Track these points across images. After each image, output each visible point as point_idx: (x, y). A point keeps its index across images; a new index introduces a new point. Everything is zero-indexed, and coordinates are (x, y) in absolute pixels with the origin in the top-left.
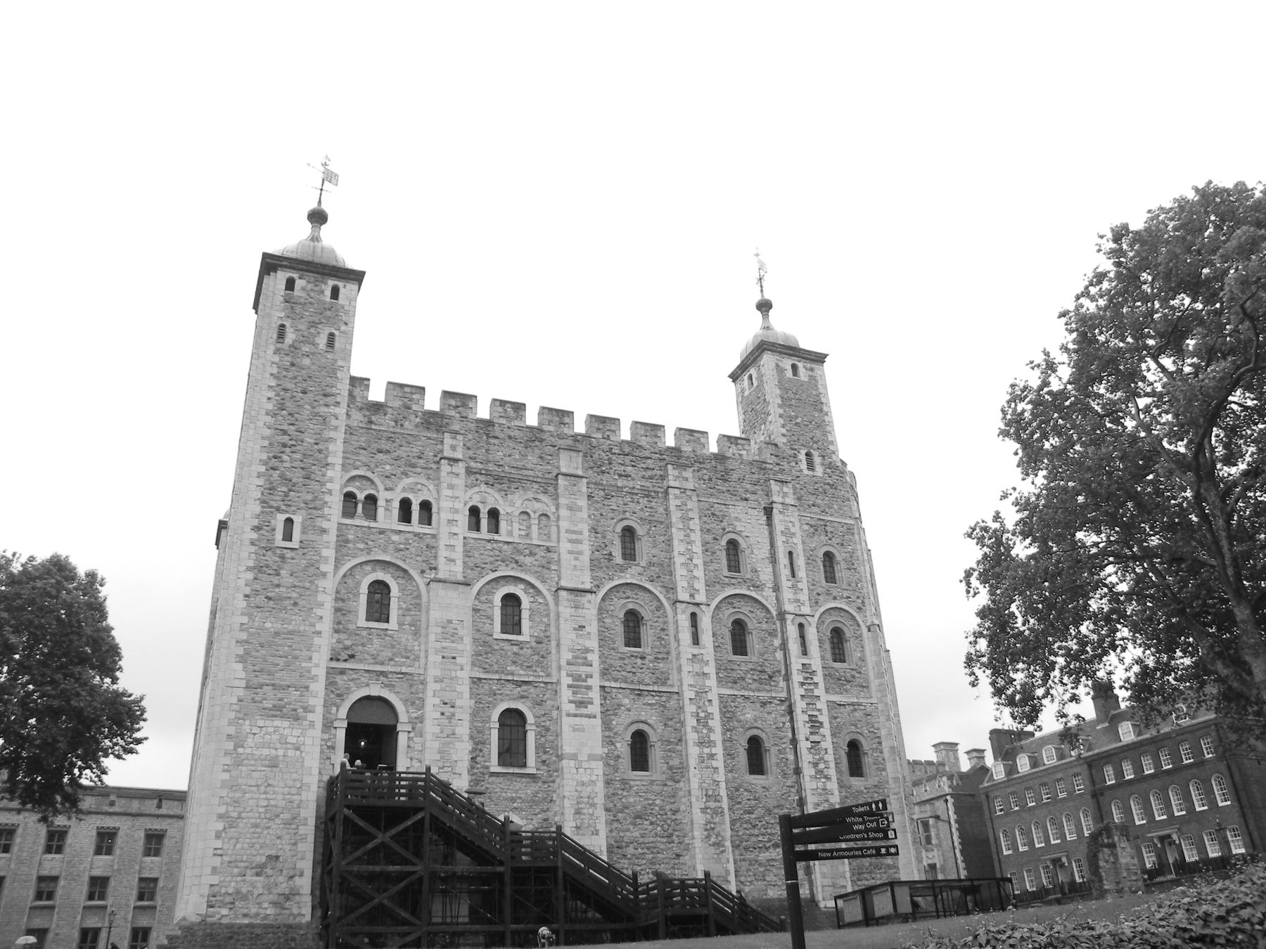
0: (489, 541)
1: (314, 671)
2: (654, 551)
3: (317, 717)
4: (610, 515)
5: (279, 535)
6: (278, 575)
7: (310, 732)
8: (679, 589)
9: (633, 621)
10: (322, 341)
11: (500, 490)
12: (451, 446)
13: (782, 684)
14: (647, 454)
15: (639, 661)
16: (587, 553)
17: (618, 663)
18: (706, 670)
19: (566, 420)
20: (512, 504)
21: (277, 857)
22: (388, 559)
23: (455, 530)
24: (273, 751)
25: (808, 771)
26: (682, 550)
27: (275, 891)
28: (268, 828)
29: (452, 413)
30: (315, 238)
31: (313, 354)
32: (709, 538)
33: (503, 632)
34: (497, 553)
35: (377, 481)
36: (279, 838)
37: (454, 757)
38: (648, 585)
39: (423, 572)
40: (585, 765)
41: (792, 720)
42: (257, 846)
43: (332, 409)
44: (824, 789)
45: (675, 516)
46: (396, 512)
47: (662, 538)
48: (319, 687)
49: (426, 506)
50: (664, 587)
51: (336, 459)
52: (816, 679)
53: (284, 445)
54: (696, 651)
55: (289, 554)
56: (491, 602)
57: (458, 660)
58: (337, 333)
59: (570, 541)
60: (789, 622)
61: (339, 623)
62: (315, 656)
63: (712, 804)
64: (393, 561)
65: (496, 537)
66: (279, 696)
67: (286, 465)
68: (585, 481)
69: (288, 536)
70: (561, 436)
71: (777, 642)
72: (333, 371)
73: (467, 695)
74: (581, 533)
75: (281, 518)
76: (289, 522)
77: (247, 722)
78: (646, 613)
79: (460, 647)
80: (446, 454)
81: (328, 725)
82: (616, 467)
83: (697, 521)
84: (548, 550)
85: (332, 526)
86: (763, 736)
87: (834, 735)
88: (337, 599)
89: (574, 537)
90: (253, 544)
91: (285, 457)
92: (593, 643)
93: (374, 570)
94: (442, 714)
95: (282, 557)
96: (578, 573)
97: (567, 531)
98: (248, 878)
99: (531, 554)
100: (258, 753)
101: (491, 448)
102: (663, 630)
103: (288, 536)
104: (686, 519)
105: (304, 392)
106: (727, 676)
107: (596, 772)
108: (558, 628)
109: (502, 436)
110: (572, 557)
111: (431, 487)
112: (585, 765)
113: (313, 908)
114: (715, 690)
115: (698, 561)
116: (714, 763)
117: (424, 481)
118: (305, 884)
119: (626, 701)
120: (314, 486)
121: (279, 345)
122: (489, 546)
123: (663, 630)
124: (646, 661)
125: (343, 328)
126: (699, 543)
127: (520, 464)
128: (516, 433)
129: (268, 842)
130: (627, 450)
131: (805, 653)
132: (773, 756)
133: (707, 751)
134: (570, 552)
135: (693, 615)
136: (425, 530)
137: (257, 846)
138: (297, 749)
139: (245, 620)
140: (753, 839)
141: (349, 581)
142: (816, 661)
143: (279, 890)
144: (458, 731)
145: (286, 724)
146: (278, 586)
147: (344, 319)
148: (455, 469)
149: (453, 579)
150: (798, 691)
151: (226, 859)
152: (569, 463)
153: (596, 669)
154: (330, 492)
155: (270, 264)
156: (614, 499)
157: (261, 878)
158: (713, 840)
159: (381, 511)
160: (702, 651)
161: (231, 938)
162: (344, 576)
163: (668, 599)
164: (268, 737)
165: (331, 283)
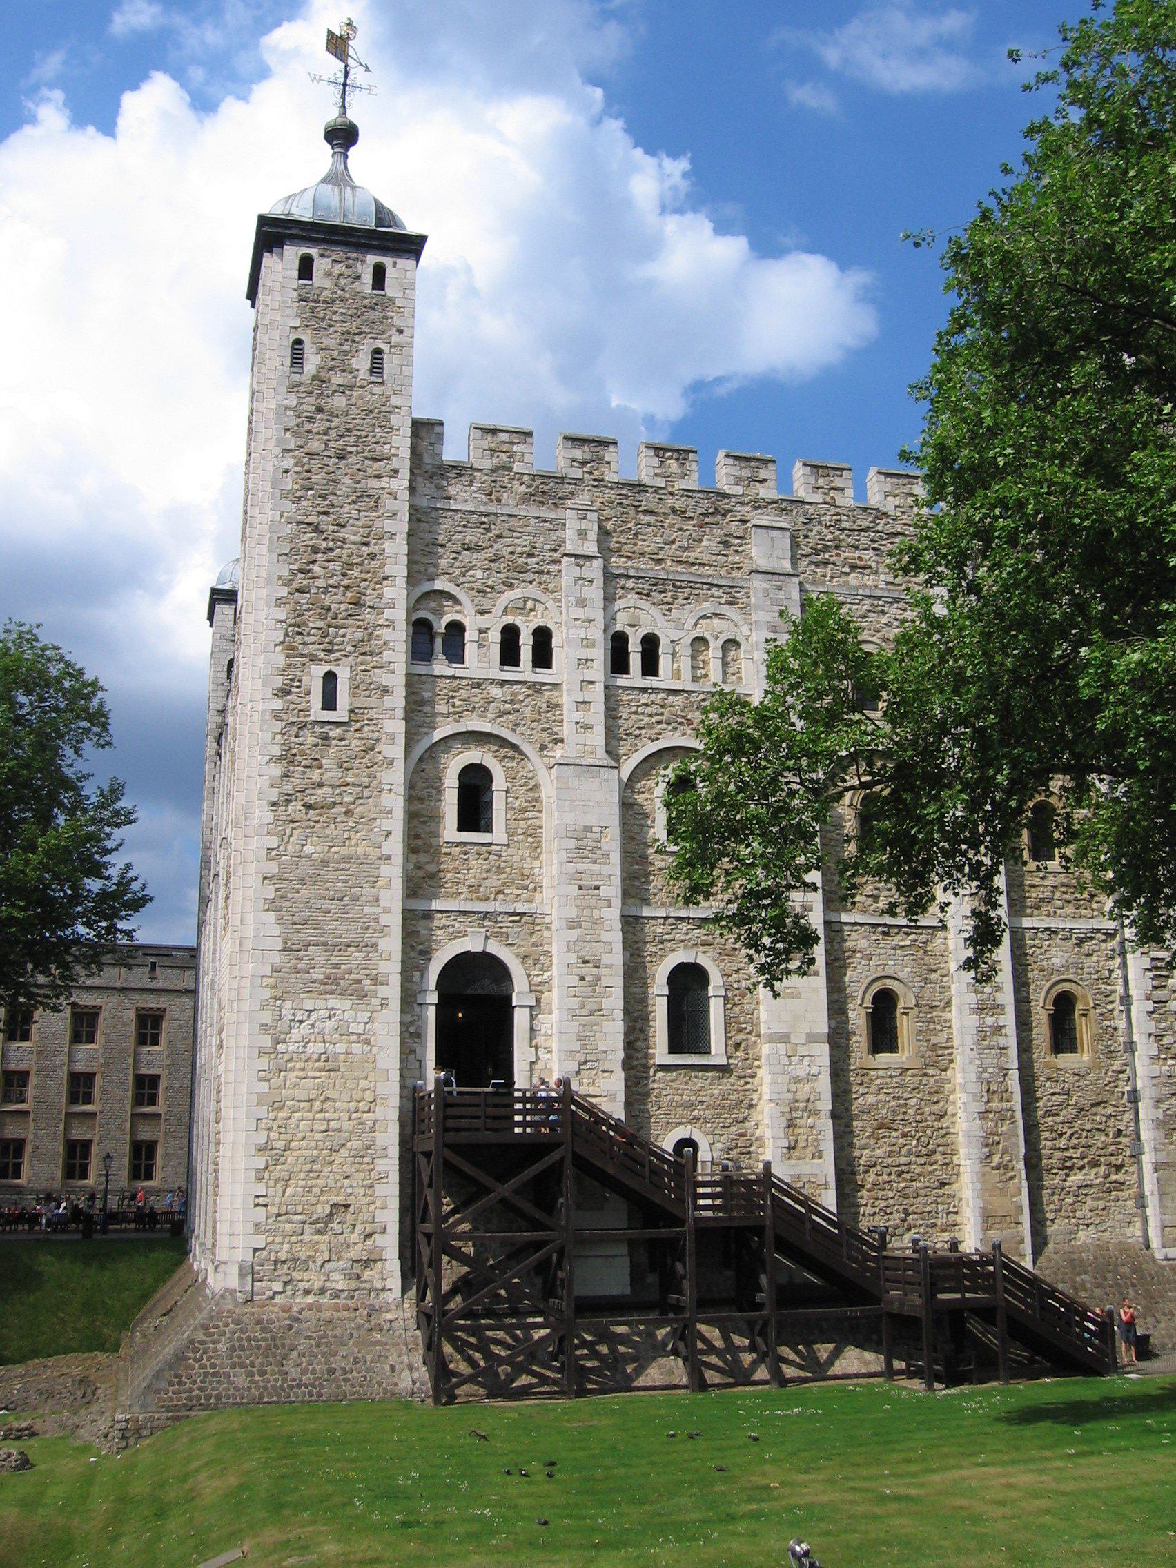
1: (384, 919)
3: (392, 991)
5: (316, 700)
6: (320, 767)
10: (362, 363)
21: (347, 1206)
27: (348, 1256)
29: (578, 473)
30: (339, 178)
31: (351, 388)
37: (602, 1046)
40: (802, 1051)
43: (385, 482)
46: (496, 651)
49: (543, 638)
51: (398, 568)
53: (315, 550)
55: (335, 732)
57: (604, 891)
58: (385, 347)
61: (417, 837)
62: (384, 895)
63: (995, 1105)
64: (496, 730)
67: (320, 582)
68: (796, 580)
69: (329, 702)
70: (757, 505)
72: (381, 416)
73: (618, 947)
75: (319, 671)
76: (330, 678)
77: (288, 1004)
79: (606, 869)
80: (569, 548)
81: (410, 999)
85: (397, 681)
90: (278, 718)
91: (317, 569)
94: (582, 979)
95: (326, 738)
98: (306, 1237)
101: (645, 530)
103: (329, 702)
105: (341, 457)
107: (819, 1061)
111: (550, 604)
112: (802, 1051)
116: (1002, 1041)
117: (533, 591)
118: (389, 1243)
120: (368, 616)
121: (296, 377)
122: (645, 698)
125: (396, 339)
127: (692, 555)
130: (864, 524)
133: (990, 1021)
136: (543, 675)
137: (316, 1190)
138: (367, 1042)
139: (273, 842)
140: (1058, 1154)
143: (353, 1254)
144: (606, 1004)
145: (347, 1004)
146: (321, 785)
147: (396, 321)
148: (586, 572)
151: (273, 1210)
154: (390, 624)
155: (273, 234)
158: (996, 1159)
159: (470, 650)
161: (290, 1327)
162: (421, 759)
165: (372, 259)
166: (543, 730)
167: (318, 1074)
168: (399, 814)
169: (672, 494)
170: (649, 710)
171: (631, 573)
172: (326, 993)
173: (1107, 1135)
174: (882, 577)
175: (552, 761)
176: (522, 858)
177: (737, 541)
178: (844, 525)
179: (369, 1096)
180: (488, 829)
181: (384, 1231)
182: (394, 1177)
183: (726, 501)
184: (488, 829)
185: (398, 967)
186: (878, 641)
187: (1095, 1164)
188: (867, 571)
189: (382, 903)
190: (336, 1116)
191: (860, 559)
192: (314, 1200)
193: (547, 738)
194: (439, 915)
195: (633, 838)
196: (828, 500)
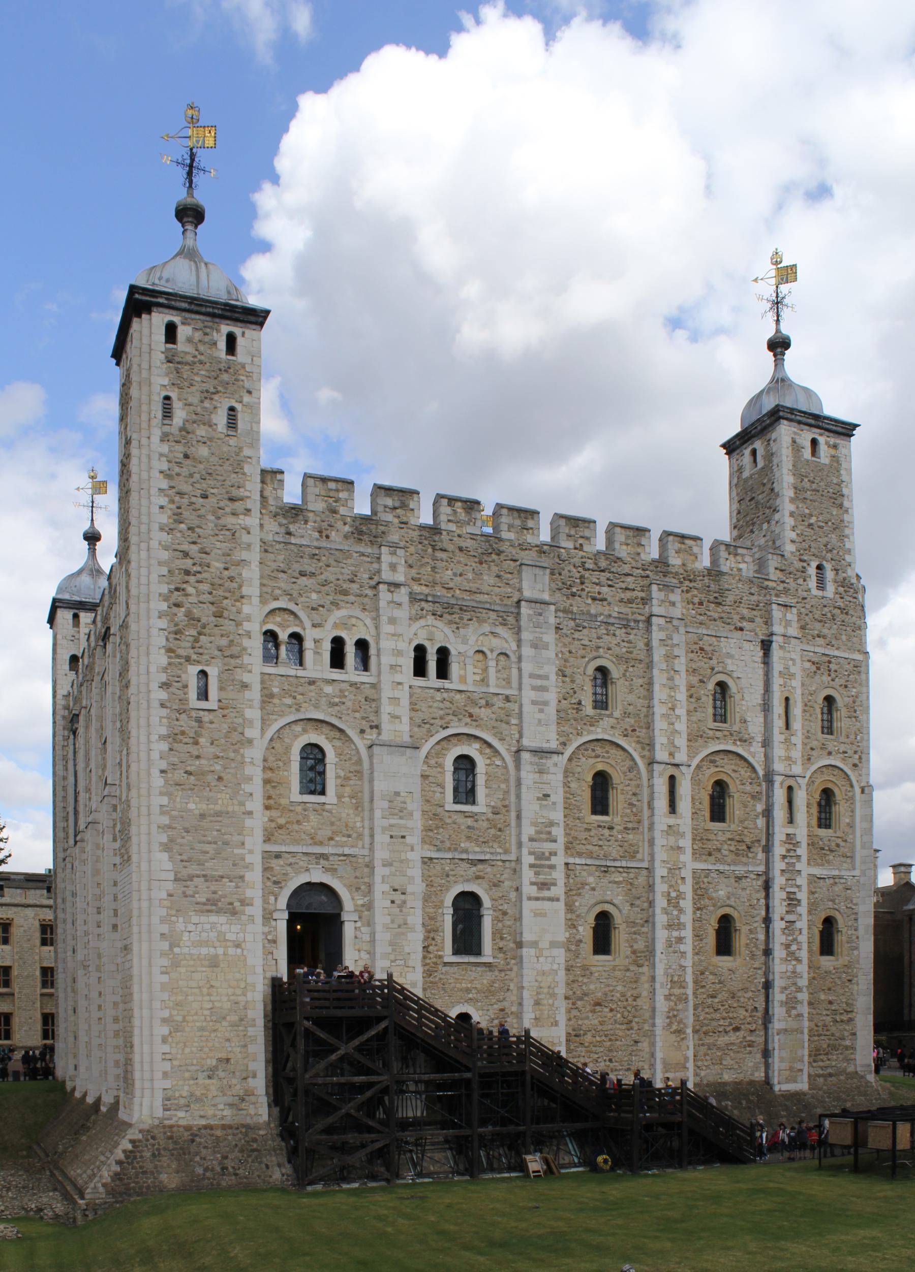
0: (438, 690)
1: (249, 859)
2: (631, 698)
3: (256, 910)
4: (581, 652)
7: (250, 928)
8: (658, 747)
9: (601, 785)
11: (450, 622)
12: (393, 565)
13: (761, 856)
14: (626, 569)
15: (606, 832)
16: (554, 703)
17: (583, 835)
18: (681, 843)
19: (530, 523)
20: (465, 641)
21: (228, 1060)
22: (321, 717)
23: (398, 678)
24: (212, 950)
25: (779, 953)
26: (664, 697)
28: (215, 1031)
32: (695, 680)
33: (456, 802)
34: (448, 704)
35: (302, 614)
36: (228, 1040)
38: (621, 742)
39: (362, 731)
41: (767, 897)
42: (206, 1049)
44: (794, 972)
45: (658, 654)
47: (640, 681)
48: (255, 876)
49: (362, 645)
50: (638, 742)
52: (799, 851)
54: (672, 821)
56: (440, 766)
59: (534, 688)
60: (777, 785)
62: (248, 841)
64: (327, 719)
65: (446, 684)
66: (213, 888)
68: (552, 608)
70: (523, 547)
71: (760, 807)
74: (546, 677)
78: (617, 778)
82: (589, 587)
83: (683, 660)
84: (507, 699)
86: (735, 914)
87: (810, 912)
88: (265, 769)
89: (539, 682)
92: (558, 815)
93: (305, 731)
96: (543, 729)
97: (531, 676)
99: (487, 704)
100: (195, 951)
101: (439, 564)
102: (634, 794)
104: (670, 657)
106: (704, 849)
108: (518, 797)
109: (450, 547)
110: (536, 708)
113: (269, 1106)
114: (689, 864)
115: (681, 711)
117: (357, 612)
118: (259, 1084)
119: (591, 879)
122: (438, 696)
123: (634, 794)
124: (615, 832)
126: (683, 689)
127: (474, 586)
128: (468, 543)
129: (217, 1045)
130: (603, 564)
131: (791, 821)
132: (743, 936)
134: (534, 703)
135: (672, 778)
138: (238, 946)
141: (277, 745)
142: (801, 830)
143: (234, 1092)
145: (223, 919)
149: (399, 741)
150: (778, 865)
152: (535, 585)
153: (560, 846)
156: (585, 631)
157: (214, 1081)
160: (678, 821)
163: (643, 757)
164: (204, 935)
166: (363, 718)
167: (204, 969)
168: (258, 780)
169: (459, 536)
170: (441, 705)
171: (430, 599)
172: (209, 911)
173: (746, 1011)
174: (616, 609)
175: (369, 742)
176: (348, 815)
177: (509, 576)
178: (587, 566)
179: (243, 985)
180: (323, 793)
181: (254, 1076)
182: (261, 1039)
183: (502, 543)
184: (323, 793)
185: (260, 893)
186: (610, 657)
187: (737, 1029)
188: (605, 603)
189: (247, 846)
190: (218, 998)
191: (599, 593)
192: (204, 1056)
193: (365, 725)
194: (287, 855)
195: (428, 801)
196: (578, 546)
